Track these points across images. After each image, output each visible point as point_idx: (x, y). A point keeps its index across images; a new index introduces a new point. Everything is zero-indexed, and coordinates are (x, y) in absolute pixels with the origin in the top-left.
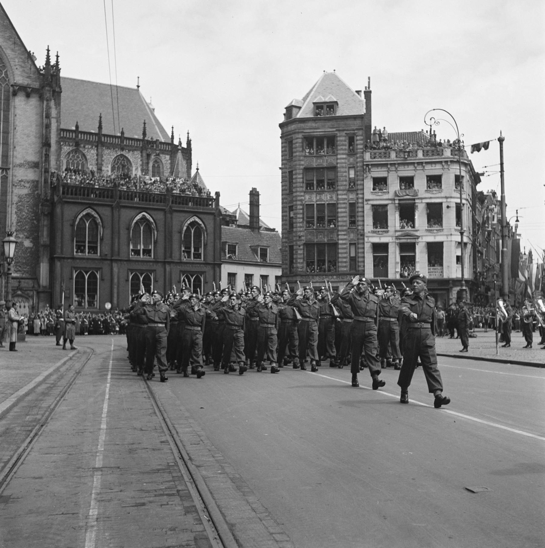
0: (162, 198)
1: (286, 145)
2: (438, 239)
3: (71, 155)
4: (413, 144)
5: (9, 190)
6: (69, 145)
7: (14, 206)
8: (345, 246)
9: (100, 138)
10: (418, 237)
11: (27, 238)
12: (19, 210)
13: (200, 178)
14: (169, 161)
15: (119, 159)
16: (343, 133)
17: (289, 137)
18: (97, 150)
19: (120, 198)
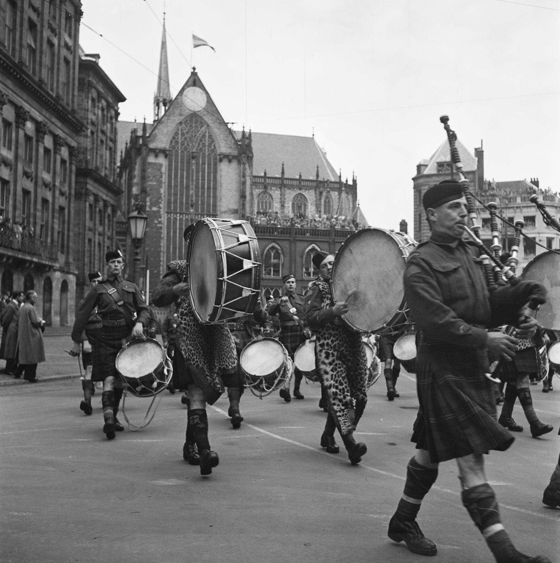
0: (326, 233)
1: (417, 194)
3: (261, 196)
4: (513, 192)
6: (260, 188)
9: (283, 181)
13: (361, 212)
14: (338, 197)
15: (298, 197)
18: (281, 191)
19: (296, 234)
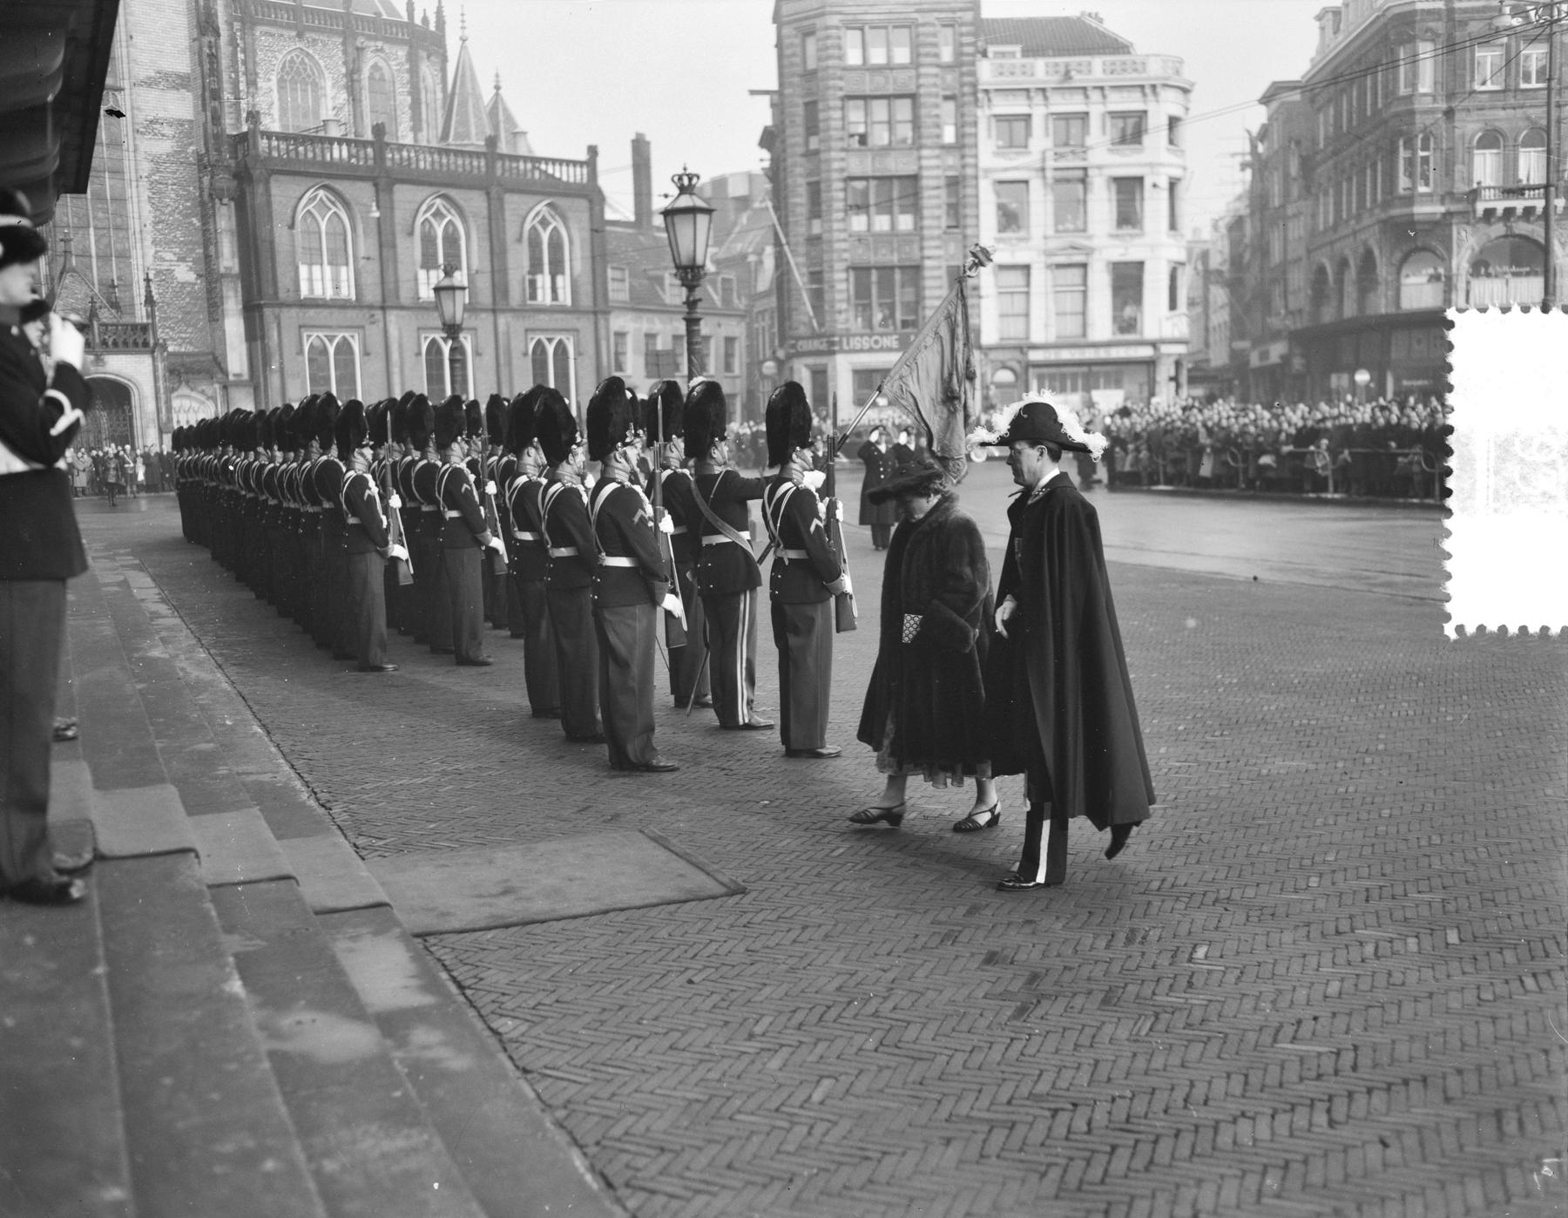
2: (1133, 255)
5: (129, 143)
7: (144, 183)
8: (936, 273)
10: (1089, 251)
11: (182, 259)
12: (156, 189)
13: (505, 109)
16: (931, 18)
17: (806, 23)
